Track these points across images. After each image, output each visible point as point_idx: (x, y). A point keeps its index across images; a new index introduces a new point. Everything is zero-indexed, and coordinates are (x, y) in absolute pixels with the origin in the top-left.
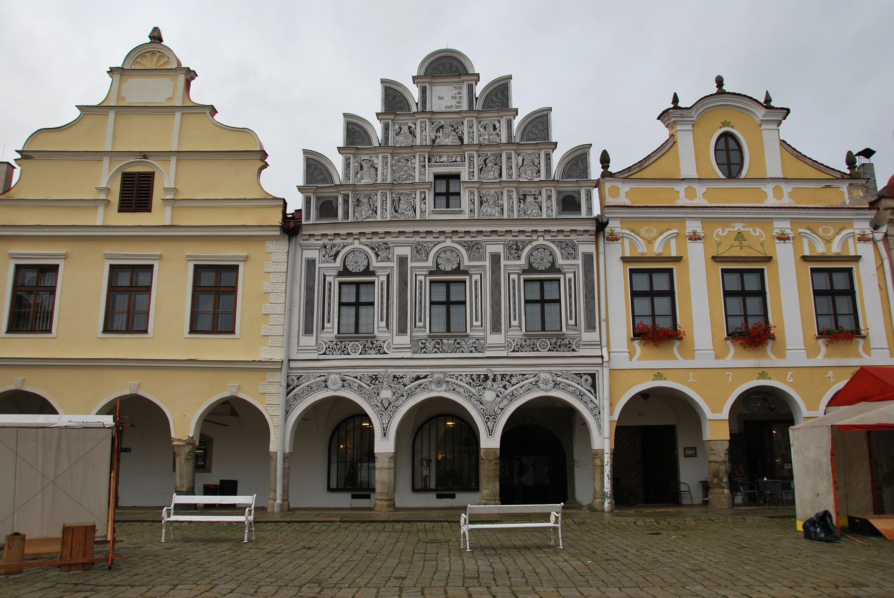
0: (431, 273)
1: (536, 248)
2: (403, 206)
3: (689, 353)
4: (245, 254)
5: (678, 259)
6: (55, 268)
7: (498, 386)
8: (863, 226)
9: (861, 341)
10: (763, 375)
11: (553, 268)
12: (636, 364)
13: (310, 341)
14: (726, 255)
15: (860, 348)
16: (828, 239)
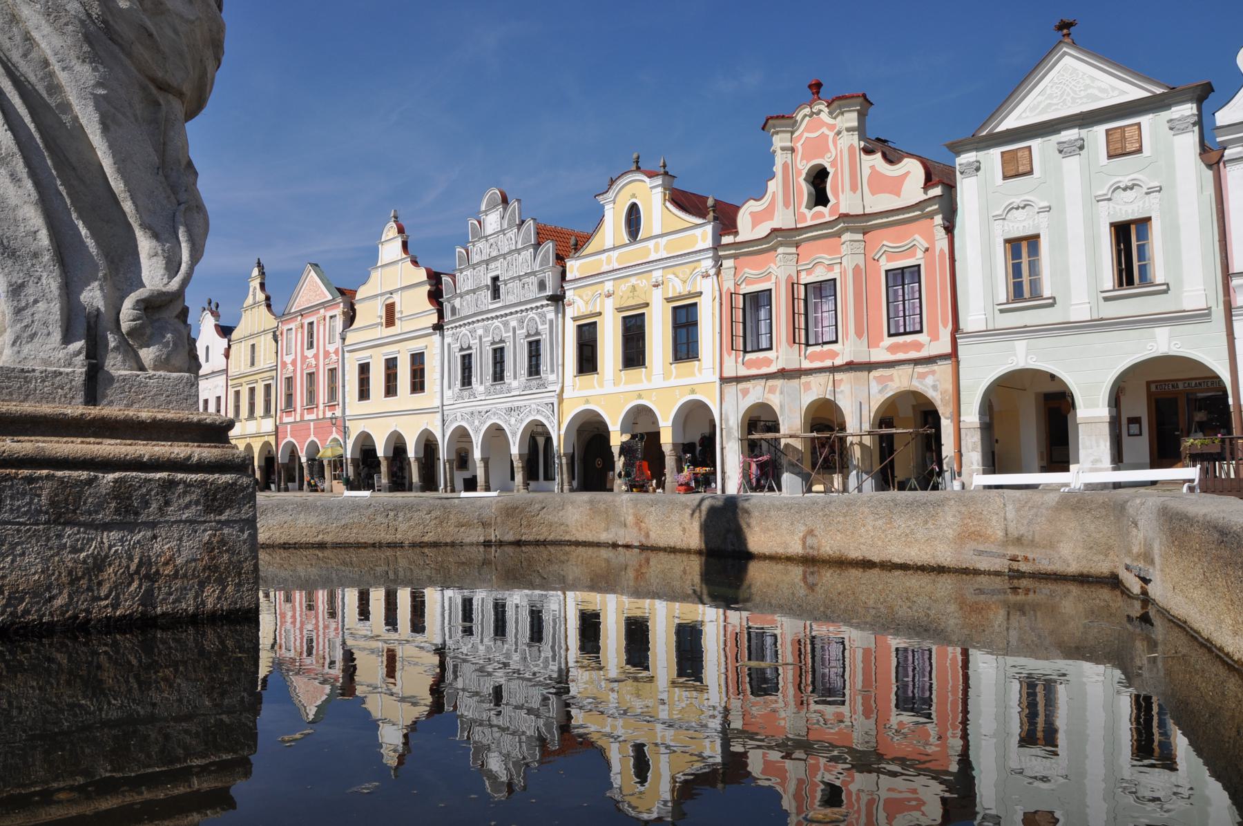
0: (492, 344)
1: (530, 320)
2: (479, 302)
3: (601, 385)
4: (424, 345)
5: (600, 314)
6: (368, 364)
7: (516, 414)
8: (707, 264)
9: (697, 363)
10: (640, 396)
11: (537, 333)
12: (577, 394)
13: (448, 393)
14: (625, 305)
15: (696, 369)
16: (684, 279)
